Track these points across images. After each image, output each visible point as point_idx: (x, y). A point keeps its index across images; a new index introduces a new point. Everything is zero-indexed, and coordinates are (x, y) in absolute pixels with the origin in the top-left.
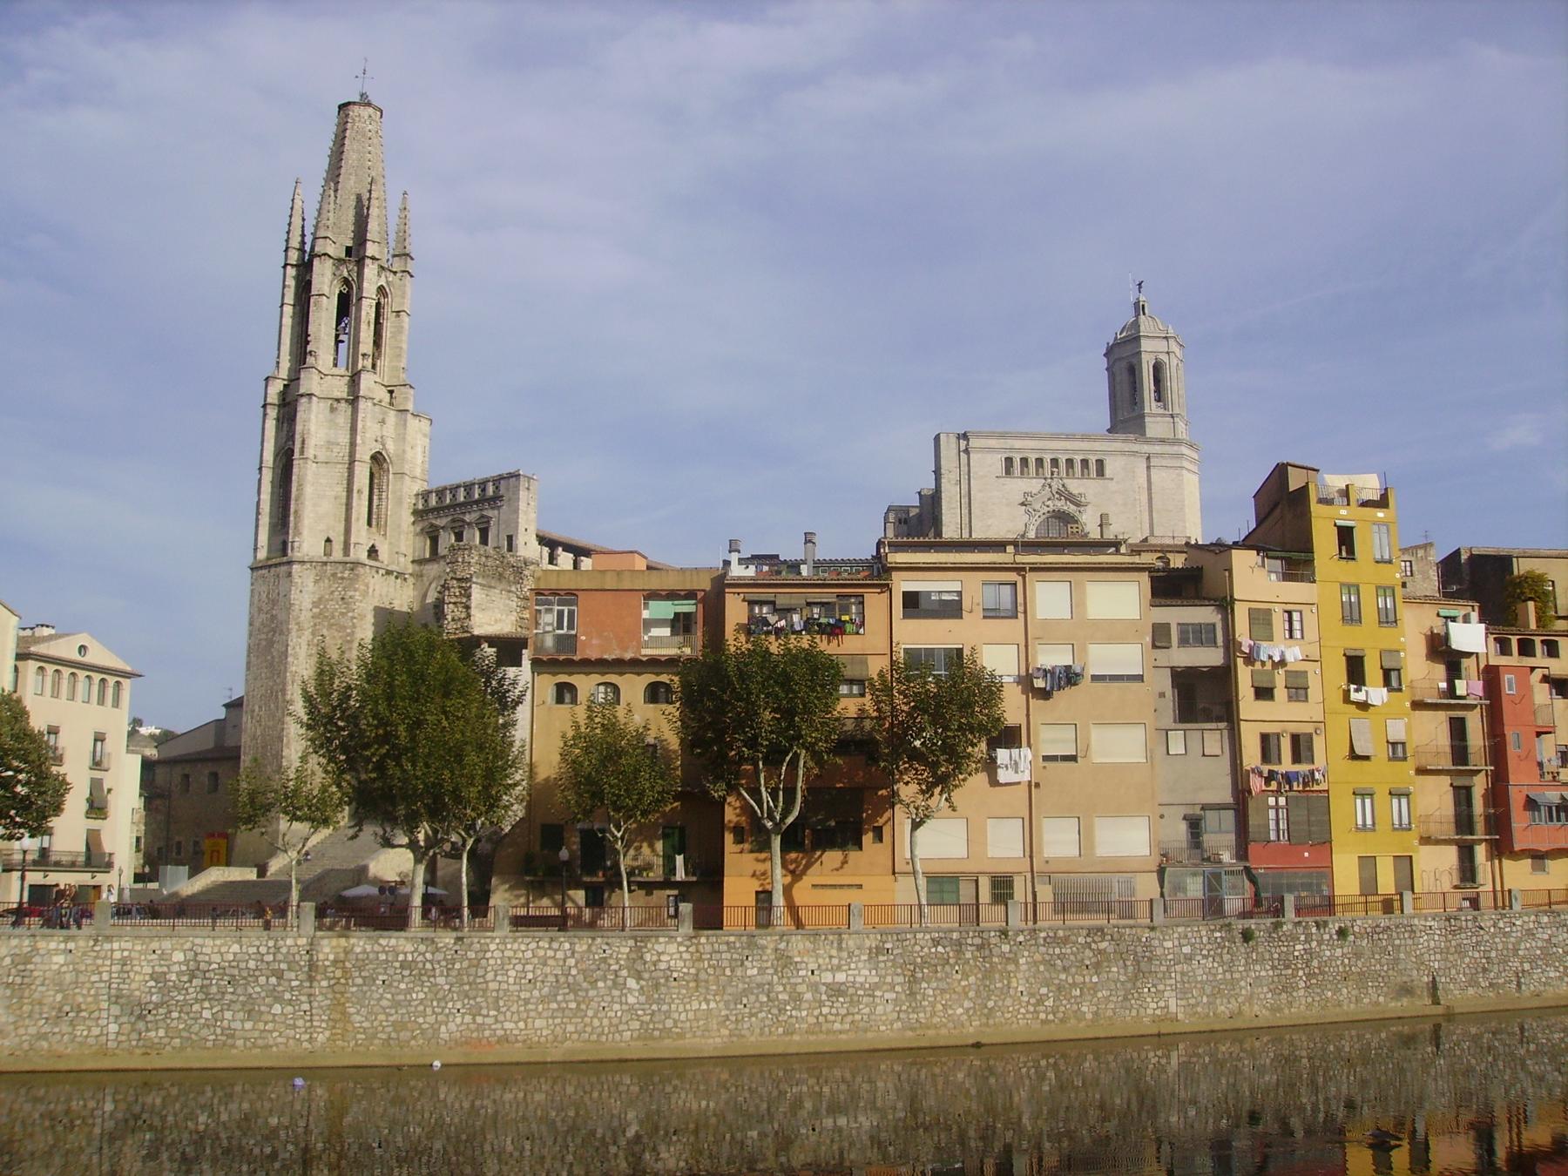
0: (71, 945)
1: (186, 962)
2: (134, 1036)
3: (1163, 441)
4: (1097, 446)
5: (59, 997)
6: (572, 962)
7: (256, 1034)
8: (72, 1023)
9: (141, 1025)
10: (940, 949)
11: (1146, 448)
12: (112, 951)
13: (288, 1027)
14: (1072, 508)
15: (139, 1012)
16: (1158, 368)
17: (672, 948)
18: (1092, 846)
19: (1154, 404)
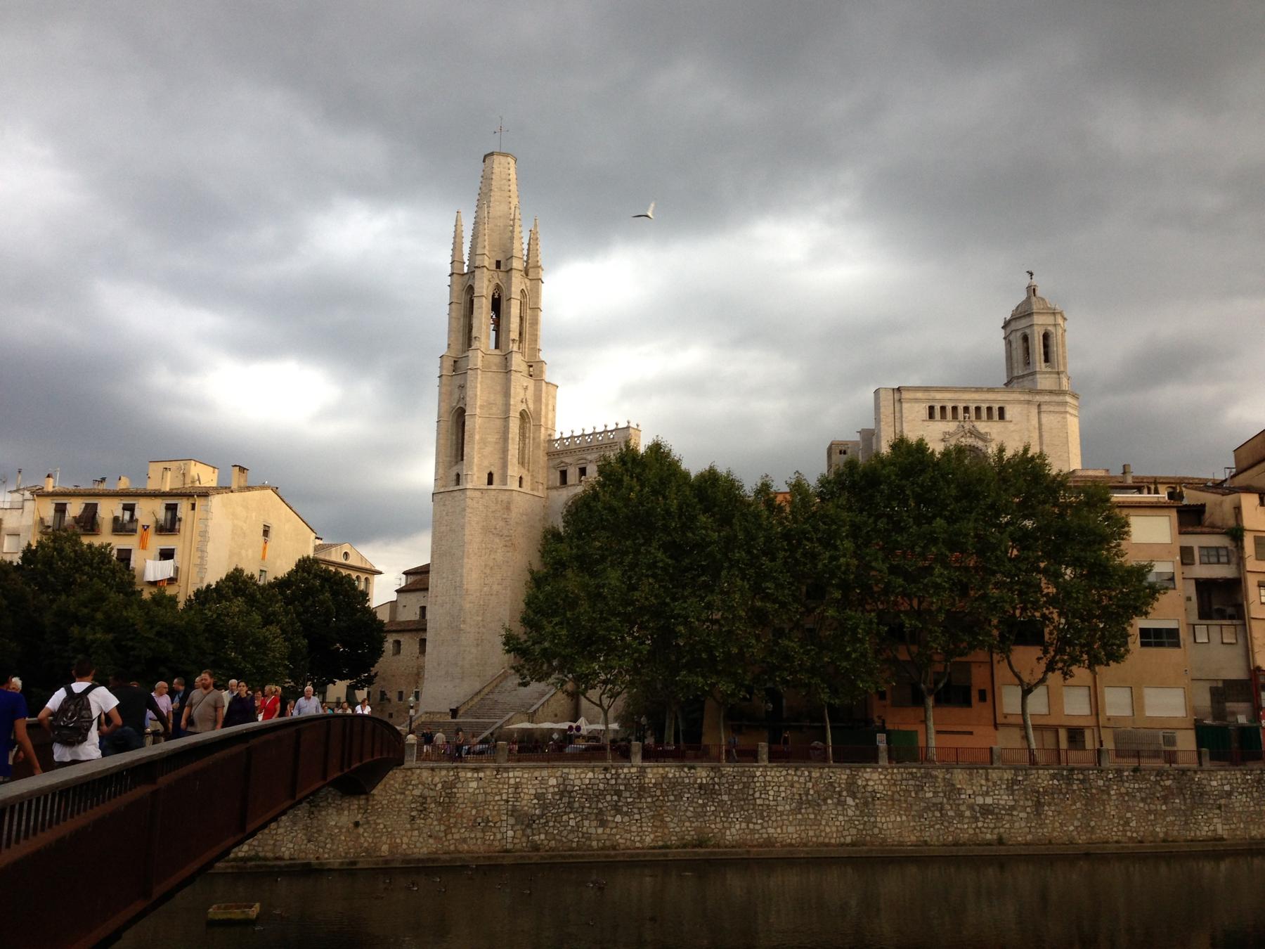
0: (482, 775)
1: (558, 785)
2: (524, 839)
3: (1051, 392)
4: (1000, 397)
5: (474, 812)
6: (810, 785)
7: (605, 837)
8: (483, 831)
9: (529, 831)
10: (1056, 782)
11: (1038, 398)
14: (980, 444)
15: (525, 821)
16: (1046, 337)
17: (875, 776)
18: (1142, 708)
19: (1043, 365)
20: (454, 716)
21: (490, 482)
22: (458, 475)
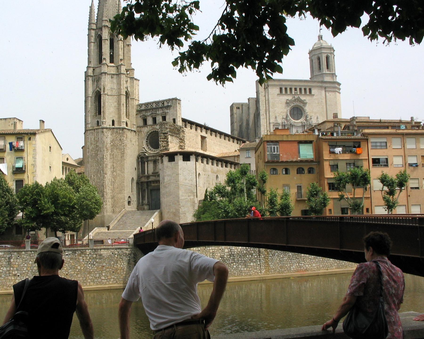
4: (309, 84)
7: (247, 271)
11: (324, 85)
12: (210, 250)
13: (255, 269)
14: (301, 105)
16: (327, 58)
20: (108, 230)
21: (113, 124)
22: (98, 122)
